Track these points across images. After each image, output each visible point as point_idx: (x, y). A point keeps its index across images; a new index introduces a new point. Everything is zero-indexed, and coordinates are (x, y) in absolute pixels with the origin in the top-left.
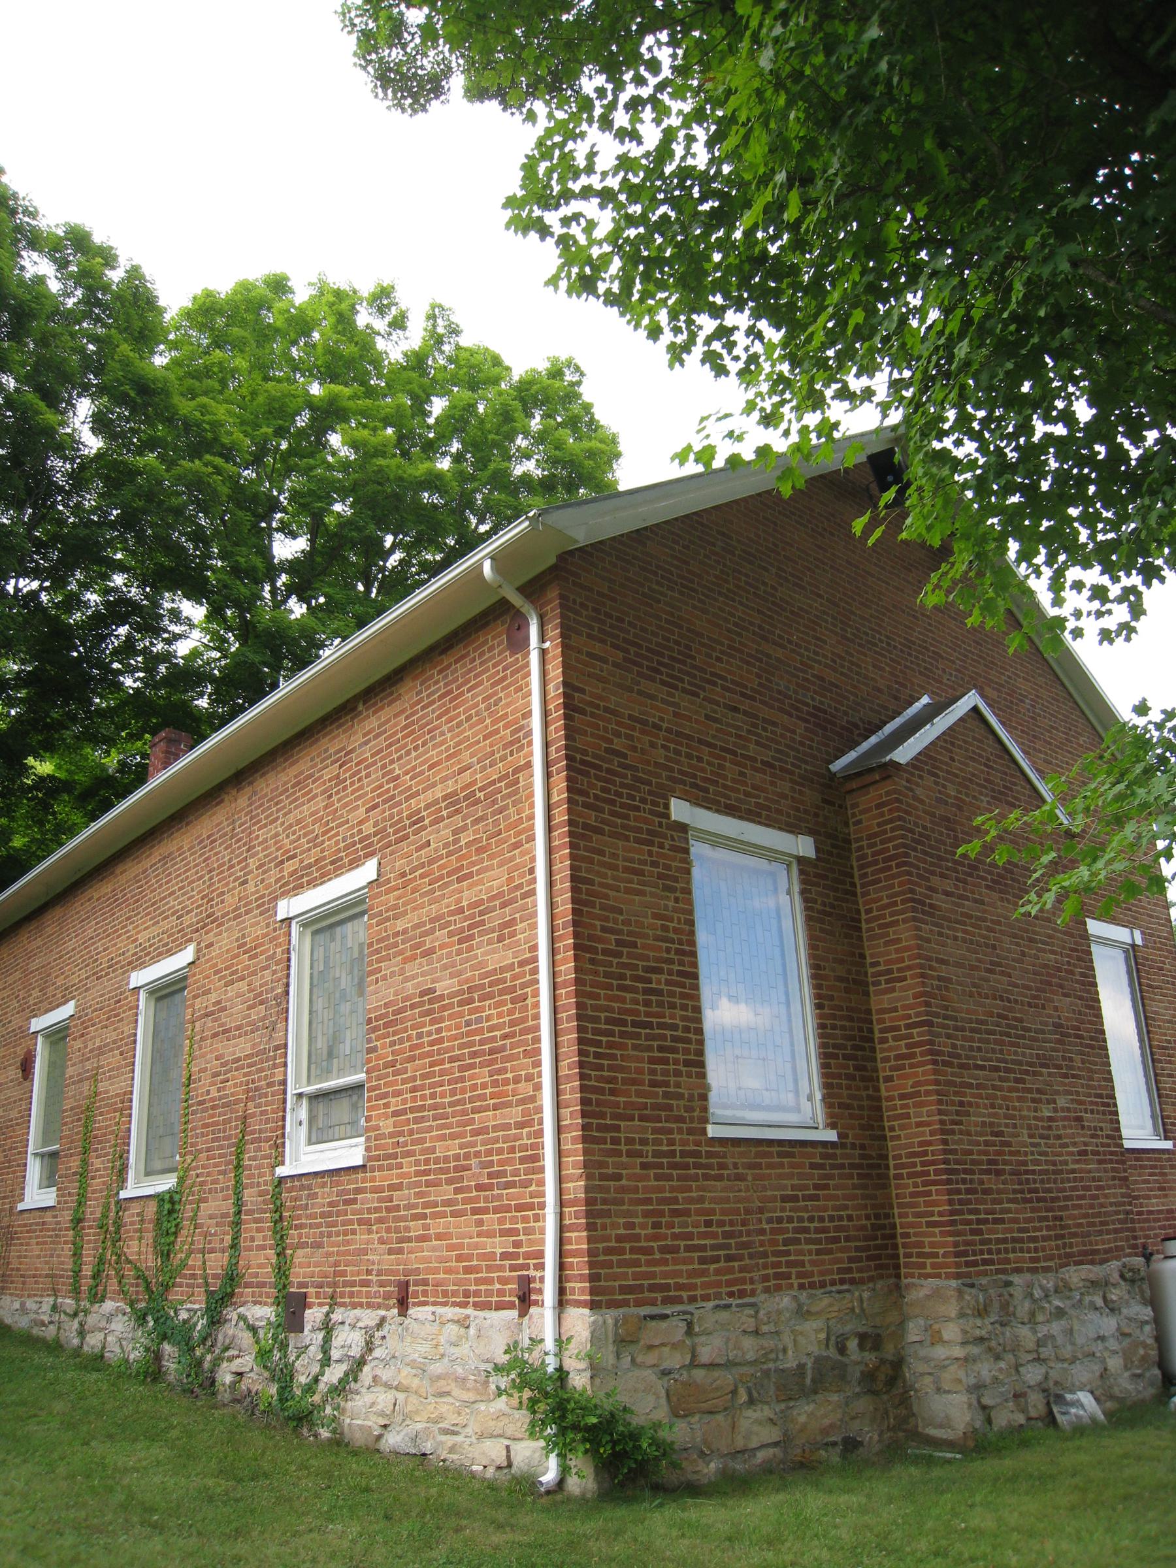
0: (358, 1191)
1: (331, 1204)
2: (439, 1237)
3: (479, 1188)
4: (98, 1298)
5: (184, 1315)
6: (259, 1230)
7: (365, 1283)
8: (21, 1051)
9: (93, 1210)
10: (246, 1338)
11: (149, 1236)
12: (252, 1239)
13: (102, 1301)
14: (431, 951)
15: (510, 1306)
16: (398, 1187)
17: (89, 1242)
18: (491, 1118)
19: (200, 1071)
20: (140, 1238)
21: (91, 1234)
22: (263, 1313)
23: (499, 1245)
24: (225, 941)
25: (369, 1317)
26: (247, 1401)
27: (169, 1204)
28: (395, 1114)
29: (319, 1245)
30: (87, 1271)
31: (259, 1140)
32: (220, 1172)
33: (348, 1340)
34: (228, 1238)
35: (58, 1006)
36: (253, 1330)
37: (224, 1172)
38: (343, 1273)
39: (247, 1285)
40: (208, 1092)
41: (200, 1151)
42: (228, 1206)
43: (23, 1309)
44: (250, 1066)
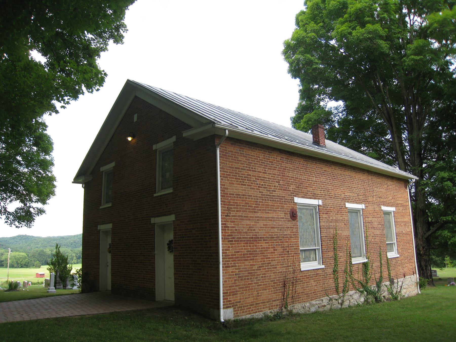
0: (398, 260)
1: (395, 263)
2: (407, 267)
3: (409, 260)
4: (345, 291)
5: (373, 288)
6: (385, 268)
7: (400, 275)
8: (288, 207)
9: (341, 268)
10: (386, 289)
11: (361, 273)
13: (348, 292)
14: (402, 226)
16: (402, 260)
17: (341, 277)
19: (369, 235)
20: (358, 273)
21: (341, 275)
22: (388, 283)
23: (411, 267)
24: (371, 208)
25: (402, 279)
27: (365, 265)
28: (401, 249)
30: (341, 285)
31: (383, 251)
32: (376, 257)
33: (400, 284)
34: (379, 270)
35: (310, 198)
36: (387, 286)
37: (377, 257)
40: (372, 240)
41: (372, 253)
42: (379, 264)
44: (380, 236)
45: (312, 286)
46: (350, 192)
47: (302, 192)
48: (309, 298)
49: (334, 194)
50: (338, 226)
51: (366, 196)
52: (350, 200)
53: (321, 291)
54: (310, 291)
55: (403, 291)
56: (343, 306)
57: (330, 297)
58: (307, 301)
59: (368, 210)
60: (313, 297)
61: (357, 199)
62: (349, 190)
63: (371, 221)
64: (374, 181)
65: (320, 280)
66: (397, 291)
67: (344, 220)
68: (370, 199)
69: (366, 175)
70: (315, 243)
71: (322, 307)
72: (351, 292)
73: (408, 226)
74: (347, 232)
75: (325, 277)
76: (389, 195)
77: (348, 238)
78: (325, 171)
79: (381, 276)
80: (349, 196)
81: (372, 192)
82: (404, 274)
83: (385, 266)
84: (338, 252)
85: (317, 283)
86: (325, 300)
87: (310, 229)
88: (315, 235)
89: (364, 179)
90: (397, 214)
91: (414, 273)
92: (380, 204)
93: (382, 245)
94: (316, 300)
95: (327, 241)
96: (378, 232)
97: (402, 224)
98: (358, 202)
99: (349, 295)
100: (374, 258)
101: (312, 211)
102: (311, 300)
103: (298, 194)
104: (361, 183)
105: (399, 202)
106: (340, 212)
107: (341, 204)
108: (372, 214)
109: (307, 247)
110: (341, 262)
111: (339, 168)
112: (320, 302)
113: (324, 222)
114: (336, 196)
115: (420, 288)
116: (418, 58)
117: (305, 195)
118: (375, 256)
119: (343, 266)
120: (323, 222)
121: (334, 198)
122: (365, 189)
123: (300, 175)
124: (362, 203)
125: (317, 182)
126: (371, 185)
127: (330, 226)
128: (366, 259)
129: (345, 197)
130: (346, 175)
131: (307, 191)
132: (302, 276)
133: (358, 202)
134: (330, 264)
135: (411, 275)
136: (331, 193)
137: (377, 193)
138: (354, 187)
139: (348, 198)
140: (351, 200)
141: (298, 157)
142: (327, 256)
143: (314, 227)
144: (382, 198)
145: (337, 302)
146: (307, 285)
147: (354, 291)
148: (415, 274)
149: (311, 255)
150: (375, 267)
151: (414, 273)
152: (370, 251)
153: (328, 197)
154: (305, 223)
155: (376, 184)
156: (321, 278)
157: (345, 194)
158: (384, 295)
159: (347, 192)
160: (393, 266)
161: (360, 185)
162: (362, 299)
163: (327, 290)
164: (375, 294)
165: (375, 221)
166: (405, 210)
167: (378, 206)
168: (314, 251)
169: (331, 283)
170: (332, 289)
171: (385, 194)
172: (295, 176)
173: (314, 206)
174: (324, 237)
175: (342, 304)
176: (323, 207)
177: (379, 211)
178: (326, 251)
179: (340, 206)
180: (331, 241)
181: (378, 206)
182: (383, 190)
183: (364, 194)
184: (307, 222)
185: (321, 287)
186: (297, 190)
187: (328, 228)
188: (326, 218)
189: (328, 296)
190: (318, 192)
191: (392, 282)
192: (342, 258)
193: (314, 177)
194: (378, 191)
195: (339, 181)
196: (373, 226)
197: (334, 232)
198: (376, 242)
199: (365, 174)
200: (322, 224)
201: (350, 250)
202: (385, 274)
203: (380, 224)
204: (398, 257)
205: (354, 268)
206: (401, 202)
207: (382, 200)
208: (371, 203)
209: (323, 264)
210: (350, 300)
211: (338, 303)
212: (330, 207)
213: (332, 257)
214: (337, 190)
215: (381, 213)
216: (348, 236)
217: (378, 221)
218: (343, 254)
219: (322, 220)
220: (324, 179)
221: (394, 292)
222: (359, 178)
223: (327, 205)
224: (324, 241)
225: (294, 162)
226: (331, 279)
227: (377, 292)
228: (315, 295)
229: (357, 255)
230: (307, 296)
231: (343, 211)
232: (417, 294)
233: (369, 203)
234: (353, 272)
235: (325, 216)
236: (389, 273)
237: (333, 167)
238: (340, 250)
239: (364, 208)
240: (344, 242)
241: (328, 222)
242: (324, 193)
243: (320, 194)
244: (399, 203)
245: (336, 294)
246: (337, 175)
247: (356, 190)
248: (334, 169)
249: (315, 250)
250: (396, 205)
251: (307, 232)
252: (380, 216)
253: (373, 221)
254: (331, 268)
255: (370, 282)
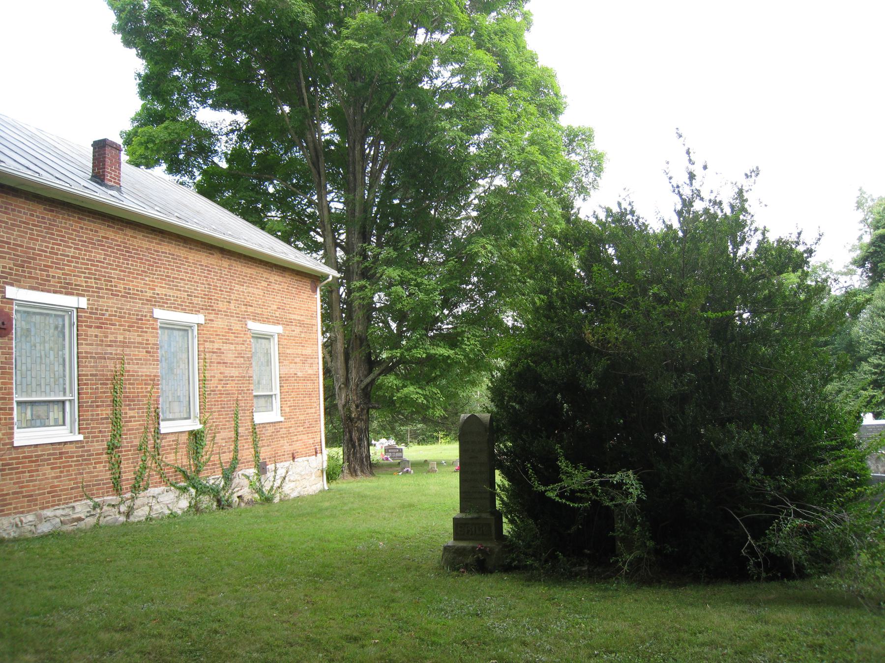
0: (281, 428)
1: (273, 432)
2: (300, 440)
3: (308, 427)
5: (212, 482)
7: (284, 455)
9: (130, 440)
11: (183, 451)
12: (244, 446)
13: (146, 489)
14: (296, 363)
15: (313, 455)
16: (291, 427)
18: (310, 411)
20: (176, 453)
22: (252, 471)
23: (311, 441)
24: (220, 323)
25: (287, 464)
26: (251, 502)
27: (196, 436)
28: (290, 407)
29: (270, 445)
30: (128, 475)
33: (281, 472)
34: (232, 447)
35: (55, 292)
36: (248, 477)
38: (277, 453)
39: (242, 463)
40: (217, 387)
41: (215, 412)
42: (232, 434)
43: (40, 519)
45: (47, 479)
46: (168, 288)
47: (30, 277)
48: (36, 505)
49: (125, 288)
50: (129, 355)
51: (211, 299)
52: (167, 303)
53: (72, 489)
54: (39, 489)
55: (287, 488)
56: (132, 519)
57: (97, 500)
58: (28, 512)
59: (213, 327)
60: (48, 502)
61: (186, 302)
62: (166, 284)
63: (220, 349)
64: (235, 270)
65: (71, 466)
66: (272, 487)
67: (146, 344)
68: (222, 306)
69: (215, 256)
70: (65, 389)
71: (72, 522)
72: (152, 491)
73: (312, 364)
74: (153, 368)
75: (86, 460)
76: (270, 301)
77: (154, 381)
78: (103, 237)
79: (235, 458)
80: (166, 295)
81: (226, 292)
82: (293, 454)
83: (247, 439)
84: (124, 409)
85: (61, 472)
86: (81, 508)
87: (52, 358)
88: (64, 371)
89: (211, 264)
90: (285, 339)
91: (316, 453)
92: (244, 318)
93: (243, 397)
94: (57, 507)
95: (96, 384)
96: (235, 372)
97: (297, 360)
98: (189, 310)
99: (148, 495)
100: (220, 422)
101: (60, 320)
102: (43, 509)
103: (19, 281)
104: (201, 272)
105: (293, 317)
106: (138, 327)
107: (141, 311)
108: (223, 335)
109: (41, 396)
110: (132, 430)
111: (143, 236)
112: (67, 511)
113: (91, 345)
114: (129, 293)
115: (328, 478)
116: (358, 45)
117: (41, 284)
118: (224, 418)
119: (135, 438)
120: (87, 344)
121: (122, 296)
122: (209, 284)
123: (30, 239)
124: (199, 312)
125: (79, 258)
126: (227, 278)
127: (106, 353)
128: (201, 423)
129: (155, 298)
130: (162, 252)
131: (48, 276)
132: (18, 458)
133: (189, 310)
134: (100, 432)
135: (309, 456)
136: (116, 286)
137: (239, 294)
138: (181, 279)
139: (162, 298)
140: (171, 303)
141: (27, 199)
142: (92, 415)
143: (64, 354)
144: (252, 306)
145: (116, 510)
146: (30, 476)
147: (163, 488)
148: (319, 455)
149: (51, 414)
150: (222, 439)
151: (316, 453)
152: (211, 408)
153: (106, 294)
154: (38, 345)
155: (239, 278)
156: (72, 461)
157: (154, 289)
158: (239, 494)
159: (161, 287)
160: (267, 440)
161: (198, 275)
162: (184, 503)
163: (87, 486)
164: (218, 492)
165: (230, 350)
166: (306, 332)
167: (239, 321)
168: (61, 405)
169: (101, 471)
170: (104, 484)
171: (260, 298)
172: (14, 240)
173: (67, 310)
174: (85, 375)
175: (128, 515)
176: (91, 313)
177: (242, 331)
178: (91, 406)
179: (137, 315)
180: (107, 384)
181: (242, 321)
182: (256, 291)
183: (204, 295)
184: (45, 342)
185: (70, 480)
186: (17, 270)
187: (101, 358)
188: (96, 336)
189: (91, 499)
190: (81, 281)
191: (262, 469)
192: (135, 421)
193: (71, 247)
194: (243, 292)
195: (141, 263)
196: (222, 360)
197: (118, 366)
198: (228, 390)
199: (213, 254)
200: (84, 348)
201: (158, 404)
202: (247, 453)
203: (242, 357)
204: (280, 422)
205: (165, 442)
206: (298, 318)
207: (250, 309)
208: (222, 315)
209: (79, 433)
210: (151, 507)
211: (119, 513)
212: (110, 315)
213: (107, 418)
214: (132, 282)
215: (245, 334)
216: (155, 376)
217: (236, 350)
218: (138, 413)
219: (85, 340)
220: (99, 254)
221: (266, 488)
222: (197, 261)
223: (101, 310)
224: (85, 384)
225: (13, 210)
226: (101, 463)
227: (223, 488)
228: (55, 497)
229: (177, 415)
230: (28, 501)
231: (146, 324)
232: (320, 491)
233: (217, 314)
234: (163, 450)
235: (93, 331)
236: (256, 452)
237: (130, 232)
238: (129, 405)
239: (203, 322)
240: (142, 388)
241: (101, 345)
242: (96, 283)
243: (95, 286)
244: (294, 319)
245: (113, 495)
246: (137, 250)
247: (187, 284)
248: (131, 236)
249: (63, 402)
250: (287, 323)
251: (41, 363)
252: (243, 341)
253: (225, 350)
254: (102, 441)
255: (207, 470)
